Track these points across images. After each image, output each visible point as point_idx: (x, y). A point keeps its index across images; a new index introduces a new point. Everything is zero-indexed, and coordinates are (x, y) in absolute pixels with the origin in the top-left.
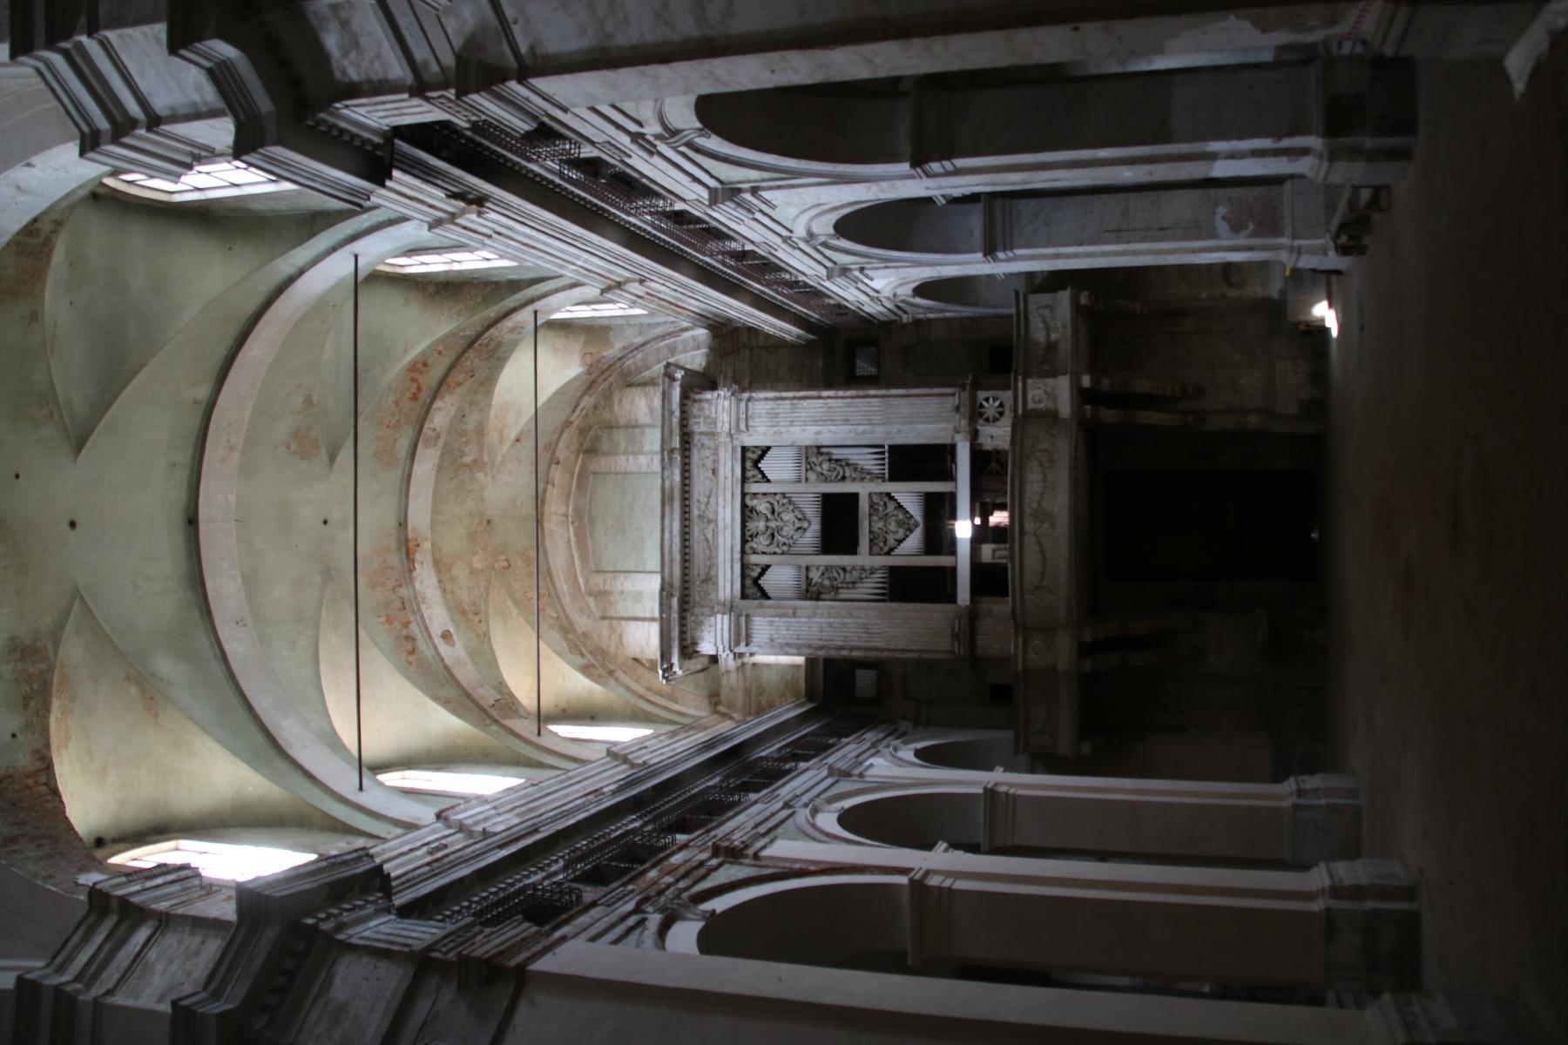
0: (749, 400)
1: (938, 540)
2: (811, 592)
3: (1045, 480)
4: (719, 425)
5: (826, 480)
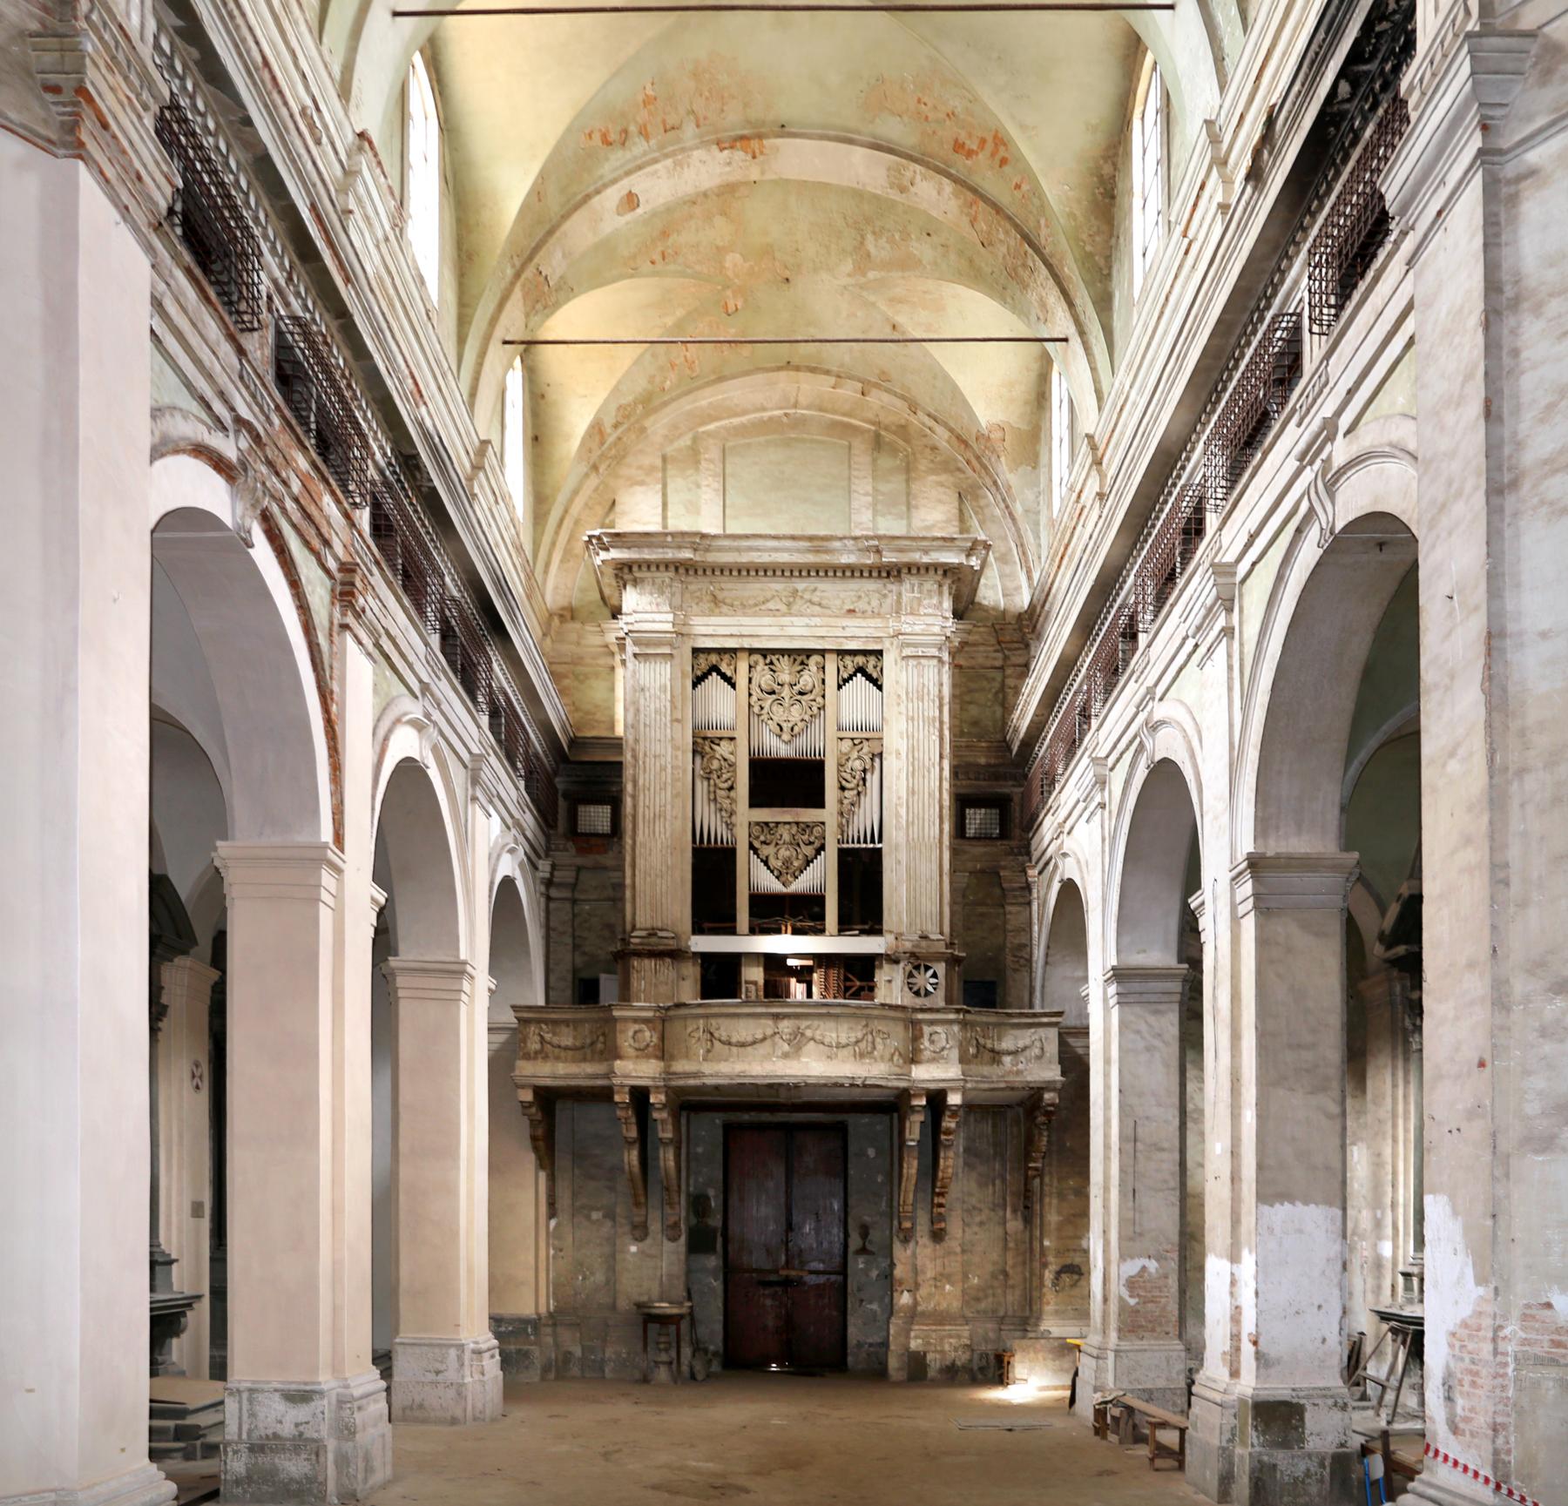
2: (703, 743)
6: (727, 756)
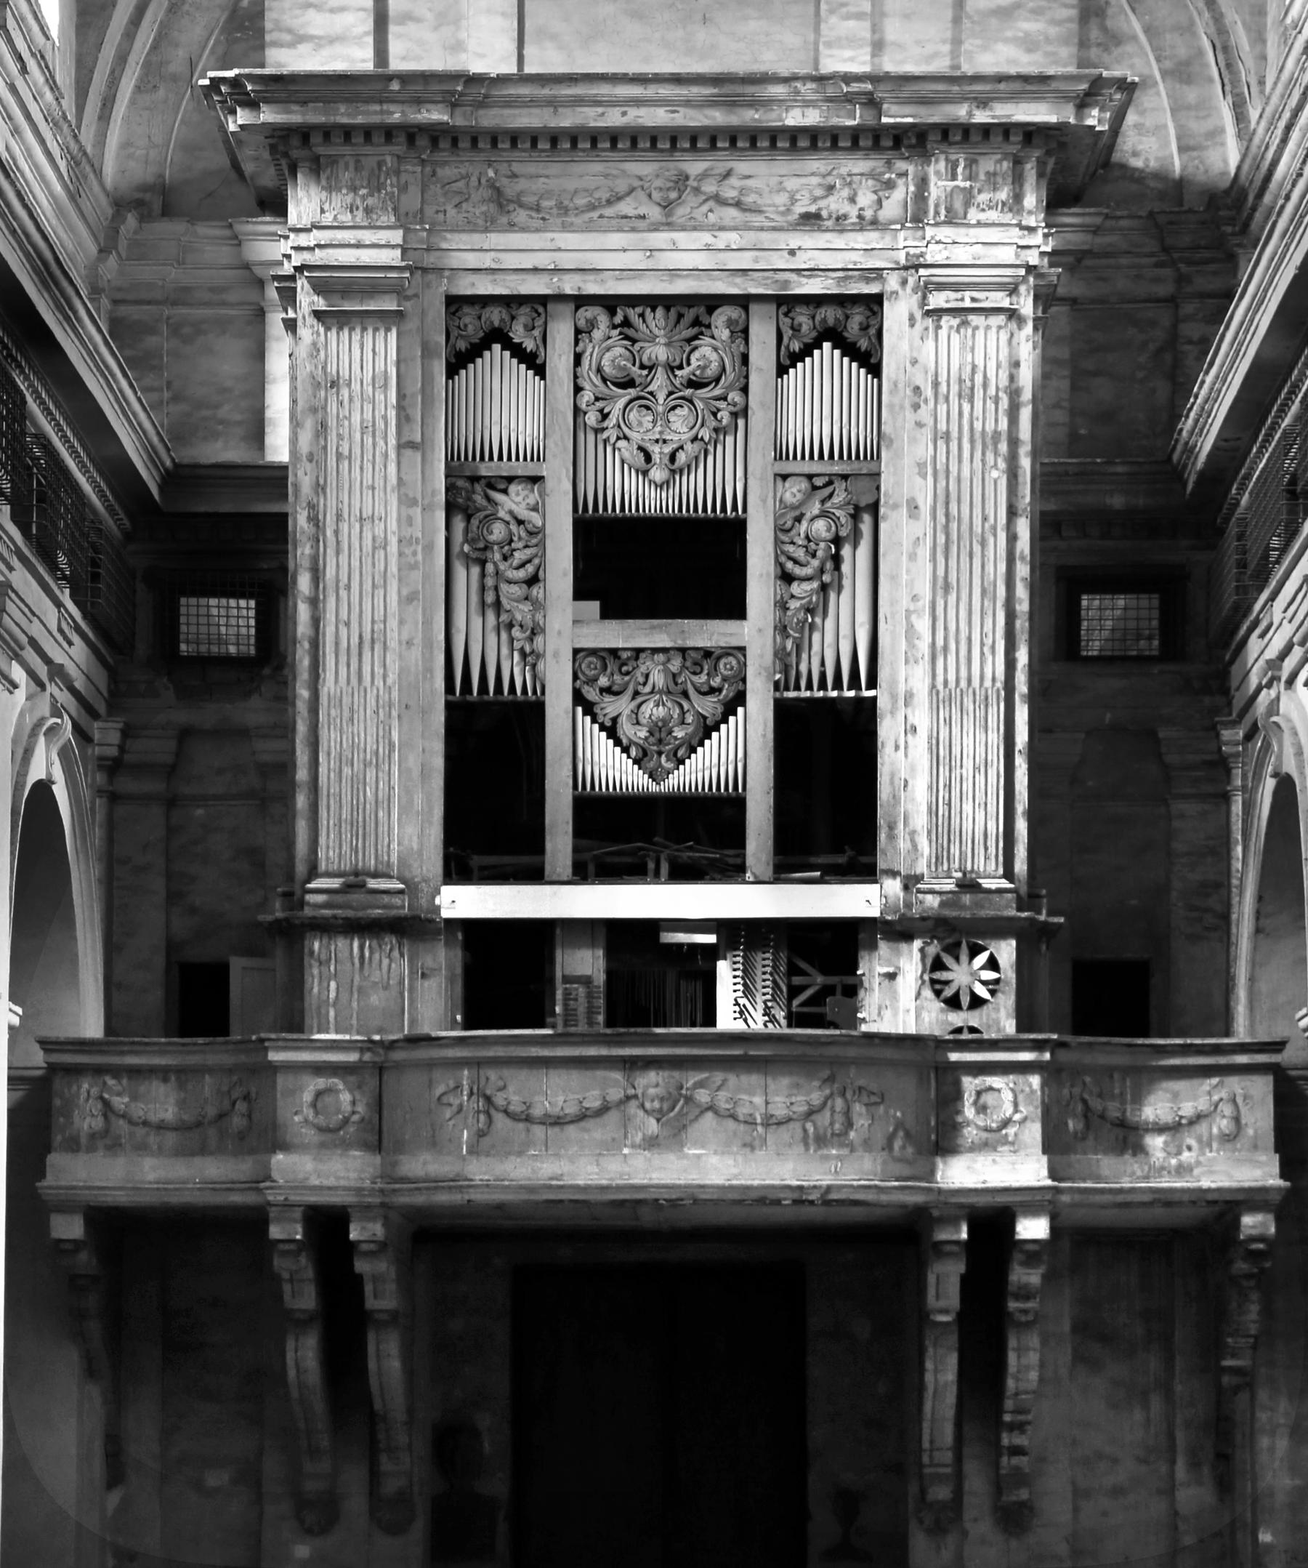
0: (1012, 314)
1: (625, 835)
2: (471, 490)
3: (771, 1122)
4: (946, 233)
5: (782, 531)
6: (523, 513)
